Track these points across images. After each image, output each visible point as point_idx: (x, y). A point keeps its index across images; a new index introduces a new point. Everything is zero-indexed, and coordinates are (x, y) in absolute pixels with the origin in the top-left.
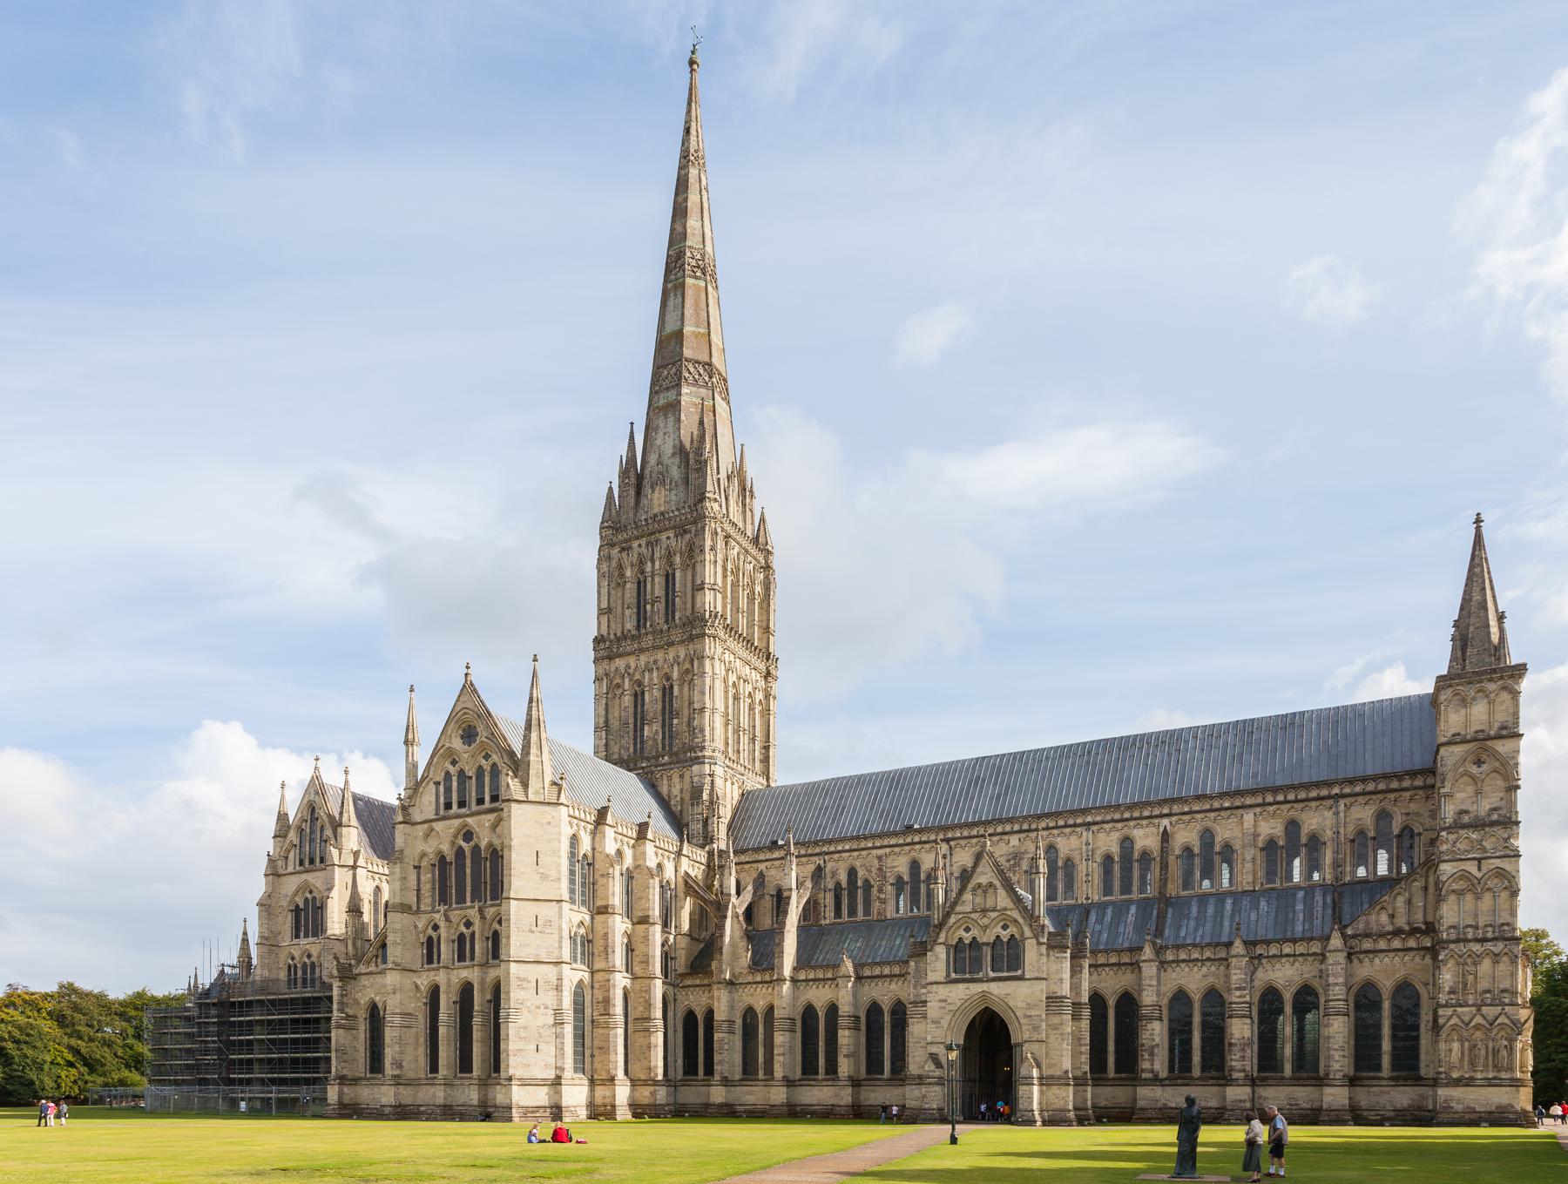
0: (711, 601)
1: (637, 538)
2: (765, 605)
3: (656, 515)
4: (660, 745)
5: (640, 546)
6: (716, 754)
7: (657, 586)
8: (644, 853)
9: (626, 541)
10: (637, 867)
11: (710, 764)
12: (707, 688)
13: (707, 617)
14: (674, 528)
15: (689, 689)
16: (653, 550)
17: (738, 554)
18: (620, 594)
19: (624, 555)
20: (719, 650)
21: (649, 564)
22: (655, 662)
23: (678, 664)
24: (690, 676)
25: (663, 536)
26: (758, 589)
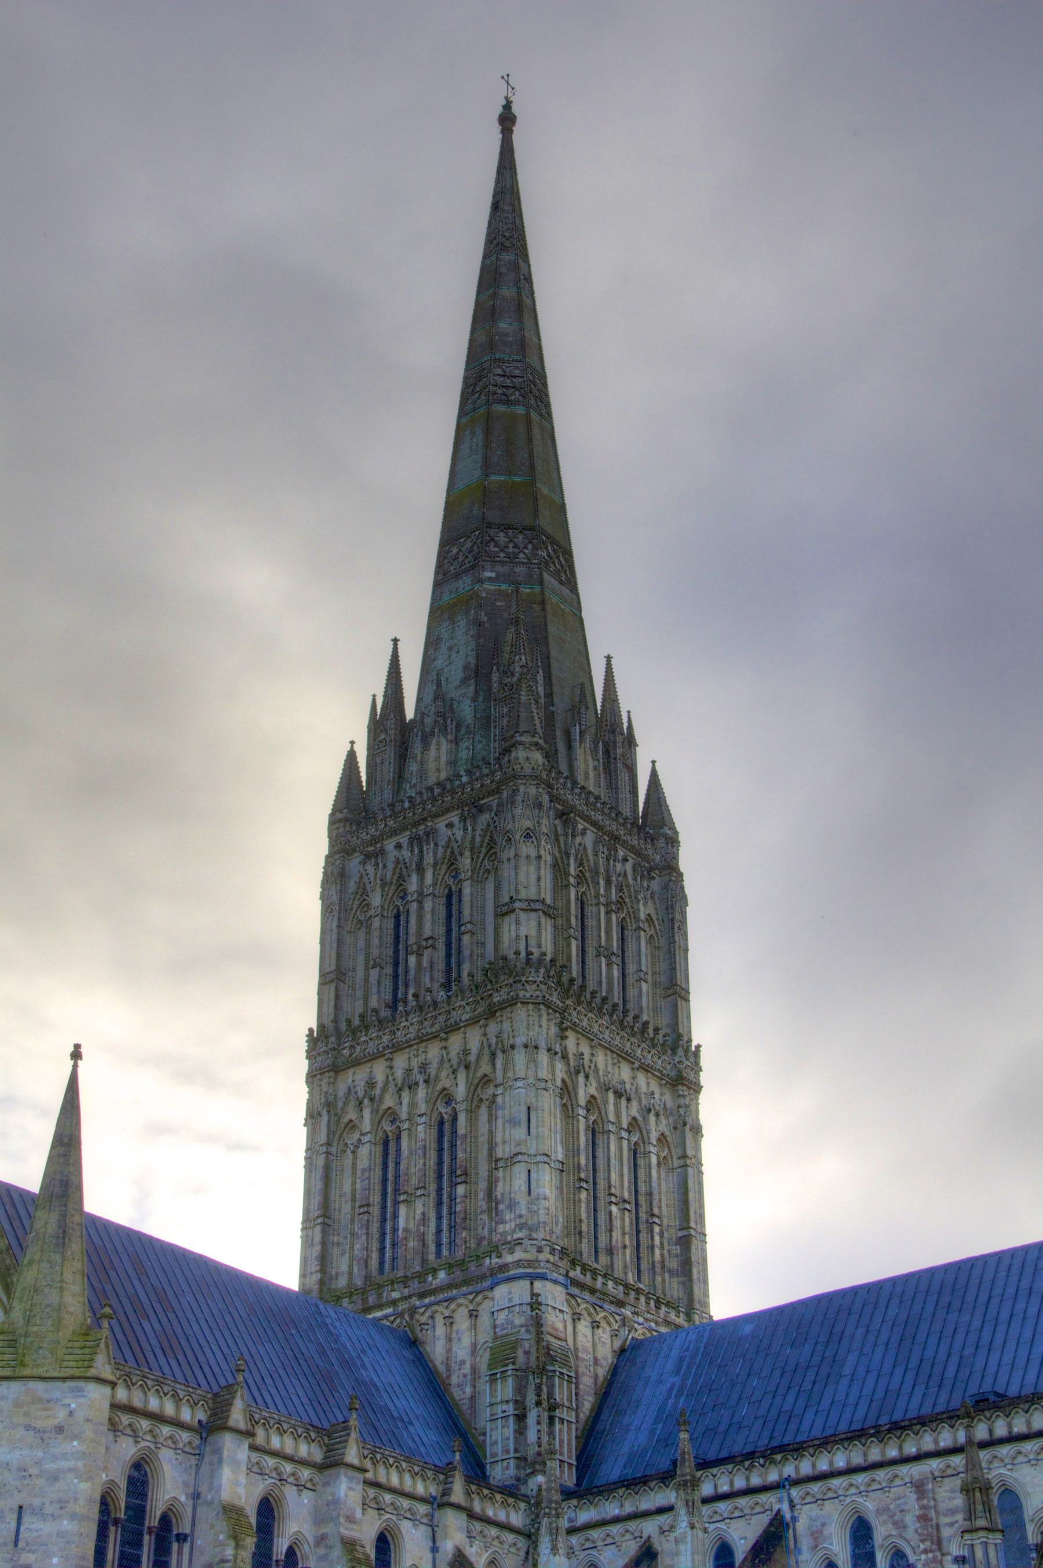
1: (394, 833)
3: (430, 789)
4: (432, 1248)
5: (399, 846)
7: (428, 916)
8: (336, 1502)
9: (374, 841)
10: (321, 1540)
11: (533, 1278)
12: (524, 1109)
14: (461, 805)
15: (490, 1116)
17: (596, 842)
18: (361, 943)
19: (370, 868)
21: (414, 878)
22: (423, 1067)
23: (467, 1067)
24: (490, 1090)
25: (441, 824)
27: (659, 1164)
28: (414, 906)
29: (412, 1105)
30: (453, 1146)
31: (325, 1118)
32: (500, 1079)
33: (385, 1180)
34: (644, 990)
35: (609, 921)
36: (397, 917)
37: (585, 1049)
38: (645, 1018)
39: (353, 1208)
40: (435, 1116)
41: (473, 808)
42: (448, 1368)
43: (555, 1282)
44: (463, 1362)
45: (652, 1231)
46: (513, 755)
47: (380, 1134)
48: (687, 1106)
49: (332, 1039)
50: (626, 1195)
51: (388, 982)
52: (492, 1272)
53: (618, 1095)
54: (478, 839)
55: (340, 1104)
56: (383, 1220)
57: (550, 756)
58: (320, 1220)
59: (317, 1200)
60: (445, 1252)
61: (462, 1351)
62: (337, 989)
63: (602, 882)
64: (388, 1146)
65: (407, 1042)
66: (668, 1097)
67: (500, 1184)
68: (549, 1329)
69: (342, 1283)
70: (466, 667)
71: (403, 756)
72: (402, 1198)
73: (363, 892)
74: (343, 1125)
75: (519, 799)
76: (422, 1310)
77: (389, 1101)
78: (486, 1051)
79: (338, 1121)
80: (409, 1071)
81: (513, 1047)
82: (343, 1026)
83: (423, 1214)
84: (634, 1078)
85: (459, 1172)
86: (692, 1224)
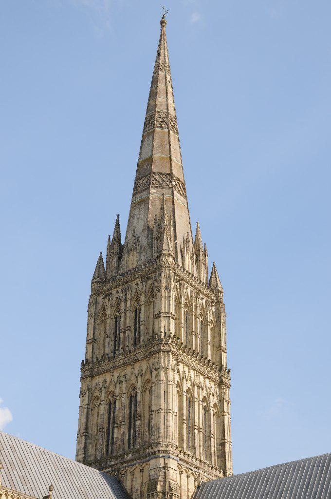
0: (167, 326)
1: (116, 287)
2: (217, 330)
3: (130, 271)
4: (127, 445)
5: (117, 292)
6: (170, 448)
12: (162, 392)
13: (162, 337)
14: (141, 277)
16: (126, 294)
17: (191, 292)
18: (103, 328)
19: (106, 300)
20: (173, 362)
21: (123, 304)
22: (125, 376)
23: (141, 376)
24: (150, 385)
25: (134, 284)
26: (210, 317)
27: (214, 415)
28: (123, 314)
29: (121, 390)
30: (135, 406)
31: (87, 394)
32: (153, 381)
33: (109, 419)
34: (209, 348)
35: (196, 322)
36: (116, 319)
37: (186, 369)
38: (209, 358)
39: (97, 429)
40: (129, 394)
41: (146, 278)
42: (132, 492)
43: (173, 459)
44: (137, 490)
45: (211, 440)
46: (161, 258)
47: (108, 401)
48: (225, 393)
49: (91, 365)
50: (201, 426)
51: (112, 344)
52: (149, 455)
53: (199, 388)
54: (147, 290)
55: (93, 389)
56: (108, 434)
57: (176, 259)
58: (84, 434)
59: (83, 427)
60: (131, 447)
61: (137, 486)
62: (93, 346)
63: (194, 307)
64: (111, 406)
65: (119, 366)
66: (217, 390)
67: (153, 421)
68: (171, 478)
69: (92, 458)
70: (144, 226)
71: (120, 258)
72: (115, 426)
73: (104, 309)
74: (94, 397)
75: (163, 275)
76: (122, 469)
77: (111, 389)
78: (149, 370)
79: (92, 396)
80: (119, 377)
81: (159, 368)
82: (95, 360)
83: (123, 432)
84: (205, 381)
85: (137, 416)
86: (226, 438)
